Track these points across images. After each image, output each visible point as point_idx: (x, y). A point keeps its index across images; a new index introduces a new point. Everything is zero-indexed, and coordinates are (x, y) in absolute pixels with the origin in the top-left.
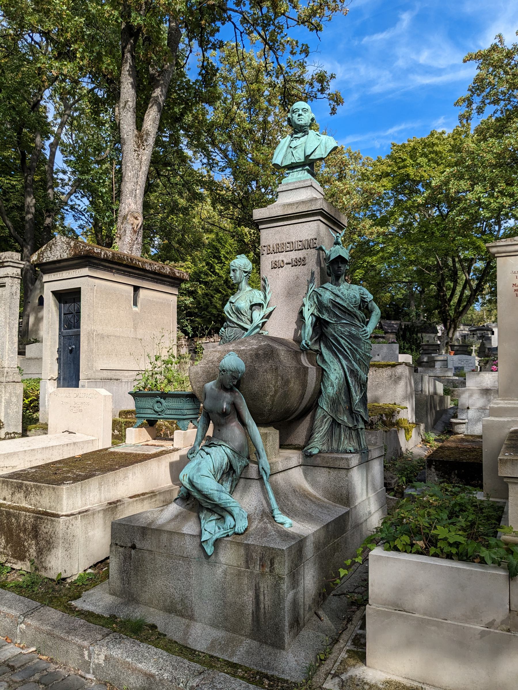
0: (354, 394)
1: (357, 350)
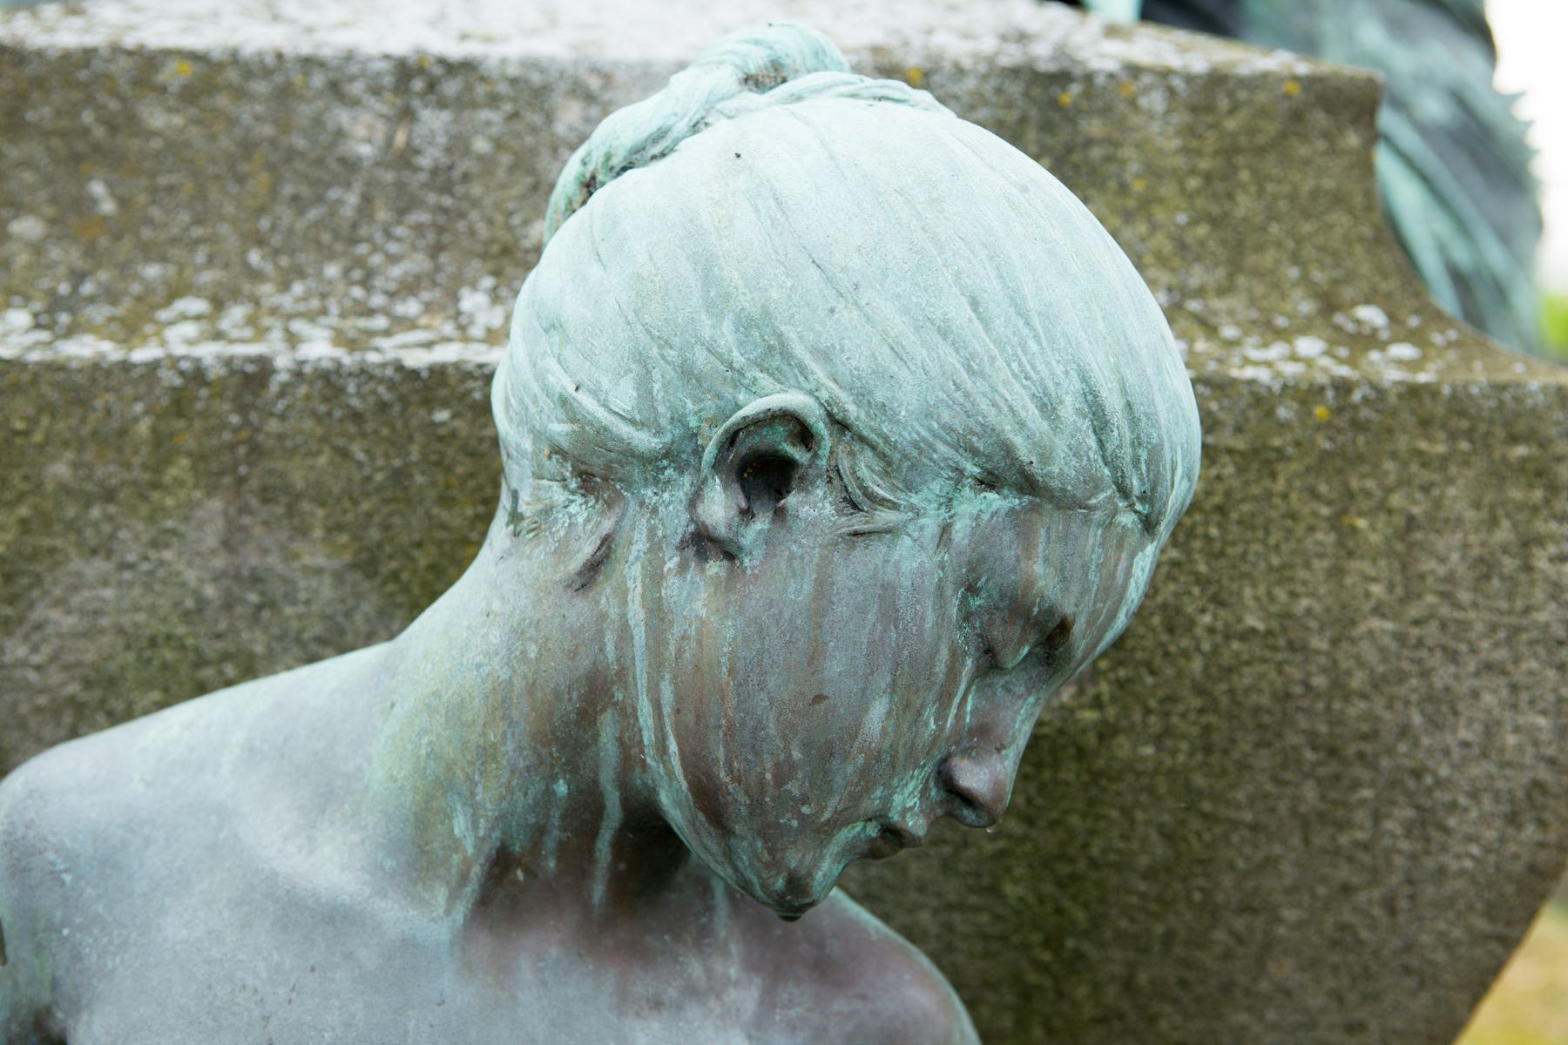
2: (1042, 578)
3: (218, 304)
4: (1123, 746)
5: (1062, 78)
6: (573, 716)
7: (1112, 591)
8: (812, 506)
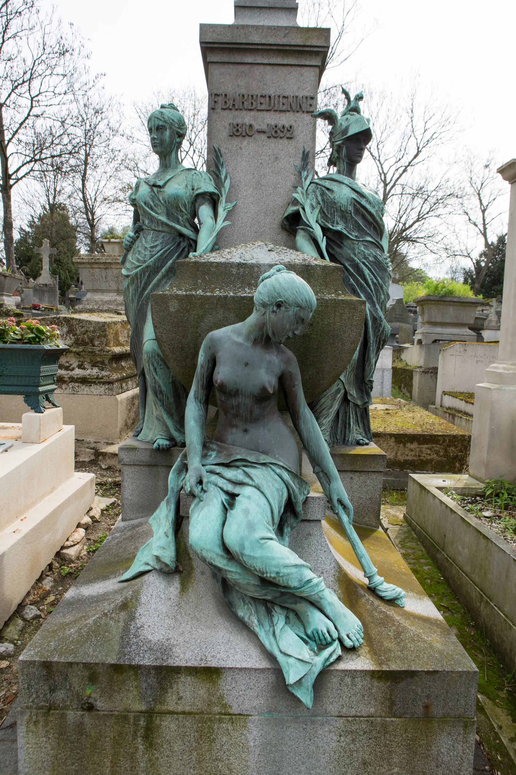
0: (372, 356)
1: (382, 287)
2: (302, 315)
3: (220, 290)
4: (312, 336)
5: (309, 266)
6: (261, 326)
7: (308, 316)
8: (283, 309)
